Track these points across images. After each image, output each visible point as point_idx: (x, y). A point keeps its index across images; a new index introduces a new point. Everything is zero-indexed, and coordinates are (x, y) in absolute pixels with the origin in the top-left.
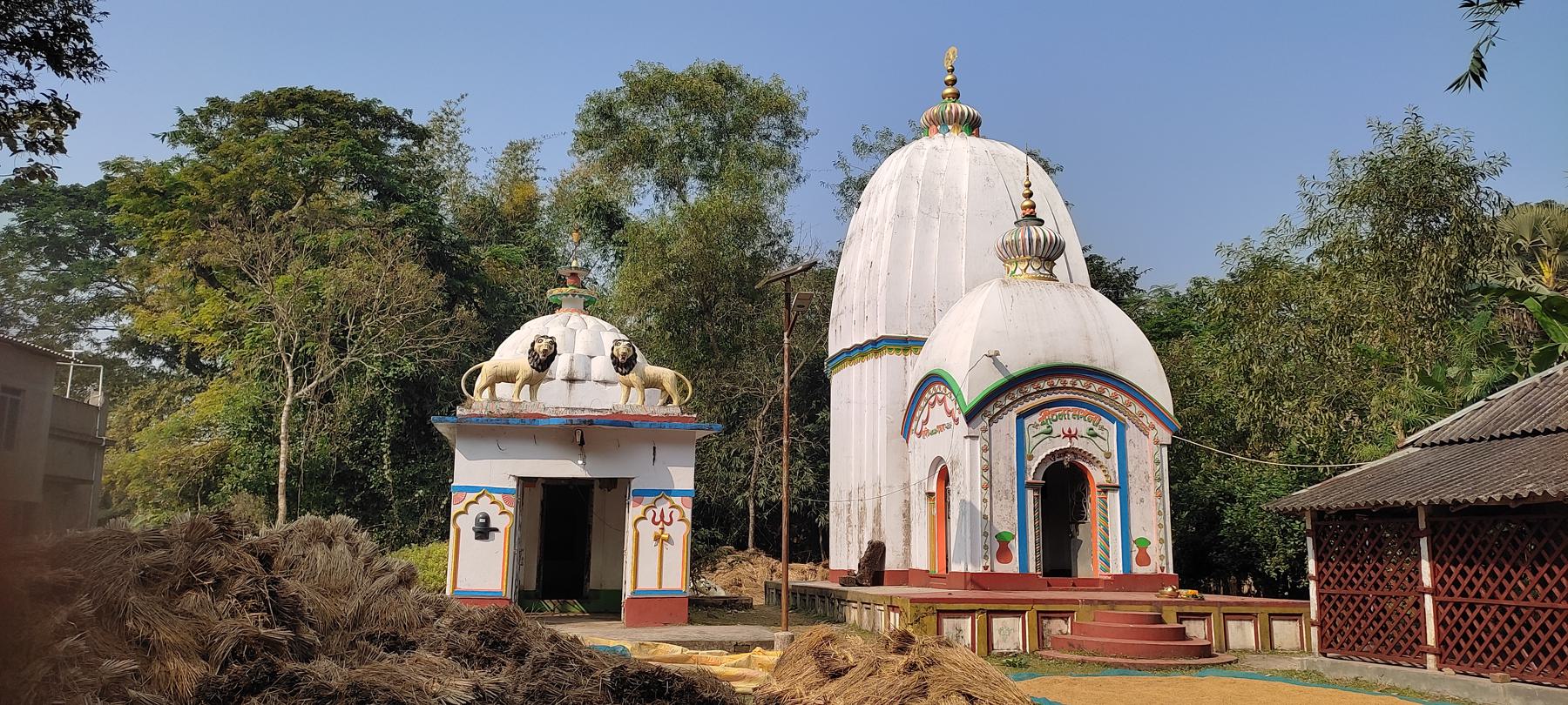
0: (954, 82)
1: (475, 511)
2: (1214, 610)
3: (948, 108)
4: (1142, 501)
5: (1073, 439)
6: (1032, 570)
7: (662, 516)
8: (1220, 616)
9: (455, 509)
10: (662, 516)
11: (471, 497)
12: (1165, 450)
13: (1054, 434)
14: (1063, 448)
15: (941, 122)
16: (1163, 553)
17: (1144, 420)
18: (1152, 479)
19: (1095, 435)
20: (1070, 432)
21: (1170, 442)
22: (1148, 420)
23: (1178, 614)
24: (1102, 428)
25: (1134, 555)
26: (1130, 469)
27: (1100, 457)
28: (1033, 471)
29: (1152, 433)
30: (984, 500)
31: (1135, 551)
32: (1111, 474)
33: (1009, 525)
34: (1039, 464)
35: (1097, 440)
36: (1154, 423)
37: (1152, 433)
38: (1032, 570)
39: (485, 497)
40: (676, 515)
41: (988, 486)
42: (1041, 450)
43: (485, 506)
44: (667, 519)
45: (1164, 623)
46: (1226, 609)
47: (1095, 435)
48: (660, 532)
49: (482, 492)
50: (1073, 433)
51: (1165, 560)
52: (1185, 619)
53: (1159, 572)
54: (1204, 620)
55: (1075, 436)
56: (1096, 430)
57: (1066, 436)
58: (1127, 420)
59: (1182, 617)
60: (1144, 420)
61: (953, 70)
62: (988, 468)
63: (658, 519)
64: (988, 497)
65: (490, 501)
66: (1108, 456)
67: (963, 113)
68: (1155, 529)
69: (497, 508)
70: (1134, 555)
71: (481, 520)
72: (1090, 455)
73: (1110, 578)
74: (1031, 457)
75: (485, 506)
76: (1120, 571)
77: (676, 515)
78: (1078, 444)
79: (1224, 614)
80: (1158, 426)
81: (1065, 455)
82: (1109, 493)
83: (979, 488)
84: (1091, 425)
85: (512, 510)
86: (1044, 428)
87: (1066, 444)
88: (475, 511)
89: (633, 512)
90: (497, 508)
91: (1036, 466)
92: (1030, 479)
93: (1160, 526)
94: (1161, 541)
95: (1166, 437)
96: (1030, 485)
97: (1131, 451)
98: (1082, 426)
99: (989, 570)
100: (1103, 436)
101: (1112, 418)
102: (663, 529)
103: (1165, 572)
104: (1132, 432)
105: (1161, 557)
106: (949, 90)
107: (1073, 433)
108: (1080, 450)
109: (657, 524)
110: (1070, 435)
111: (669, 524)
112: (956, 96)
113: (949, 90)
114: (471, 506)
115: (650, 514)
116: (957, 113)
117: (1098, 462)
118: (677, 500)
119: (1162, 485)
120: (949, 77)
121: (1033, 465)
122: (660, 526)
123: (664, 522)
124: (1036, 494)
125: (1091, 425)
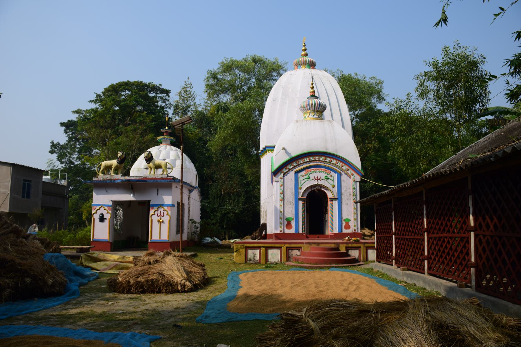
0: (305, 50)
1: (99, 212)
2: (362, 246)
3: (300, 59)
5: (319, 180)
7: (161, 213)
8: (364, 248)
9: (93, 212)
10: (161, 213)
11: (98, 208)
13: (311, 179)
14: (314, 184)
15: (298, 65)
17: (349, 172)
19: (328, 179)
20: (317, 178)
22: (351, 172)
23: (346, 247)
24: (331, 176)
27: (330, 187)
28: (302, 194)
29: (352, 177)
30: (281, 205)
34: (304, 191)
35: (329, 180)
37: (352, 177)
39: (102, 208)
40: (166, 213)
41: (283, 200)
42: (305, 185)
43: (102, 211)
44: (162, 215)
45: (340, 251)
46: (366, 245)
47: (328, 179)
48: (159, 219)
49: (102, 206)
50: (319, 178)
52: (350, 249)
54: (358, 249)
55: (319, 179)
56: (329, 177)
57: (316, 179)
58: (341, 172)
59: (348, 249)
60: (349, 172)
61: (305, 46)
62: (283, 193)
63: (159, 215)
64: (282, 204)
65: (104, 209)
67: (306, 61)
69: (106, 212)
71: (101, 216)
72: (326, 186)
74: (301, 189)
75: (102, 211)
77: (166, 213)
78: (321, 182)
79: (366, 247)
80: (355, 174)
81: (316, 187)
83: (279, 201)
84: (326, 175)
85: (110, 212)
87: (316, 183)
88: (99, 212)
89: (151, 212)
90: (106, 212)
91: (303, 191)
92: (300, 197)
95: (358, 178)
98: (323, 175)
100: (332, 179)
102: (161, 218)
104: (344, 177)
106: (303, 53)
107: (319, 178)
108: (322, 185)
109: (159, 216)
110: (318, 179)
111: (163, 216)
112: (306, 55)
113: (303, 53)
114: (98, 211)
115: (156, 213)
116: (304, 61)
118: (166, 208)
120: (303, 48)
121: (302, 191)
122: (160, 217)
123: (161, 216)
125: (326, 175)
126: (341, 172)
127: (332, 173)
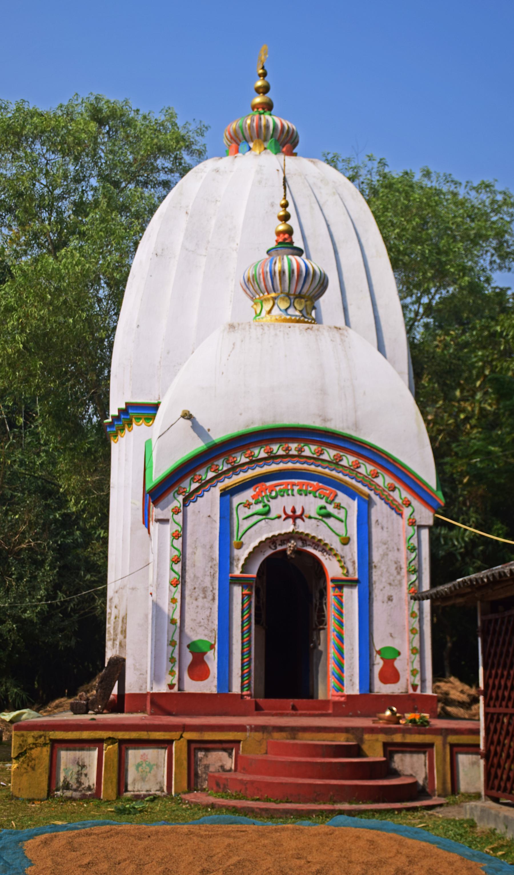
4: (390, 599)
6: (236, 689)
12: (425, 534)
13: (273, 515)
16: (417, 666)
18: (404, 571)
19: (328, 515)
20: (294, 511)
21: (431, 522)
25: (377, 670)
26: (376, 557)
27: (335, 543)
28: (242, 562)
29: (407, 512)
31: (379, 664)
32: (349, 565)
33: (206, 632)
36: (410, 497)
37: (407, 512)
38: (236, 689)
47: (328, 515)
50: (298, 512)
51: (418, 677)
53: (411, 691)
55: (301, 517)
56: (330, 509)
57: (288, 517)
58: (372, 493)
60: (395, 495)
66: (346, 541)
68: (407, 635)
70: (377, 670)
72: (320, 540)
73: (343, 699)
74: (240, 546)
76: (355, 690)
78: (303, 527)
80: (416, 503)
82: (346, 590)
86: (259, 508)
87: (288, 527)
92: (237, 572)
93: (413, 631)
94: (414, 651)
96: (236, 580)
97: (377, 534)
99: (175, 690)
101: (351, 493)
103: (418, 692)
105: (414, 672)
107: (298, 512)
108: (307, 535)
117: (331, 549)
119: (419, 578)
121: (242, 554)
124: (246, 592)
125: (322, 503)
126: (372, 493)
127: (342, 498)
